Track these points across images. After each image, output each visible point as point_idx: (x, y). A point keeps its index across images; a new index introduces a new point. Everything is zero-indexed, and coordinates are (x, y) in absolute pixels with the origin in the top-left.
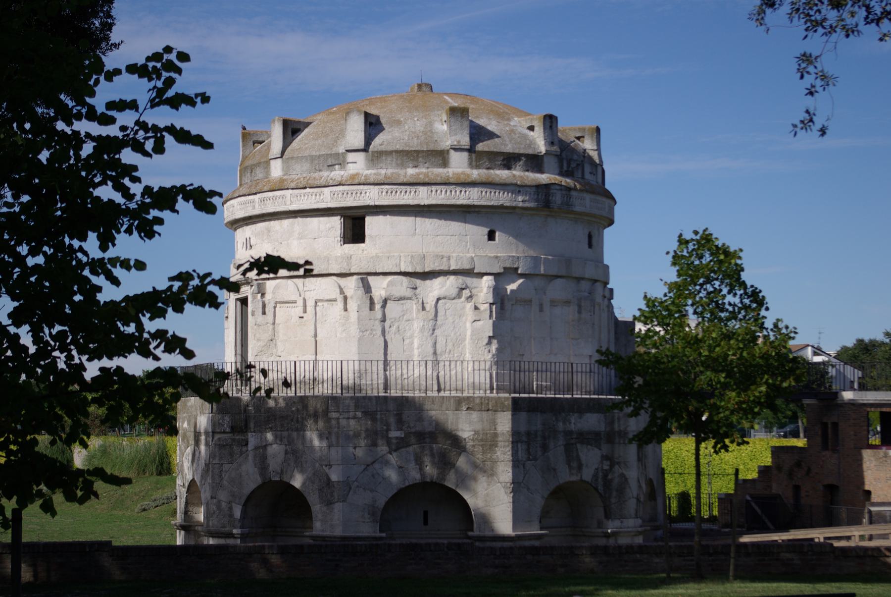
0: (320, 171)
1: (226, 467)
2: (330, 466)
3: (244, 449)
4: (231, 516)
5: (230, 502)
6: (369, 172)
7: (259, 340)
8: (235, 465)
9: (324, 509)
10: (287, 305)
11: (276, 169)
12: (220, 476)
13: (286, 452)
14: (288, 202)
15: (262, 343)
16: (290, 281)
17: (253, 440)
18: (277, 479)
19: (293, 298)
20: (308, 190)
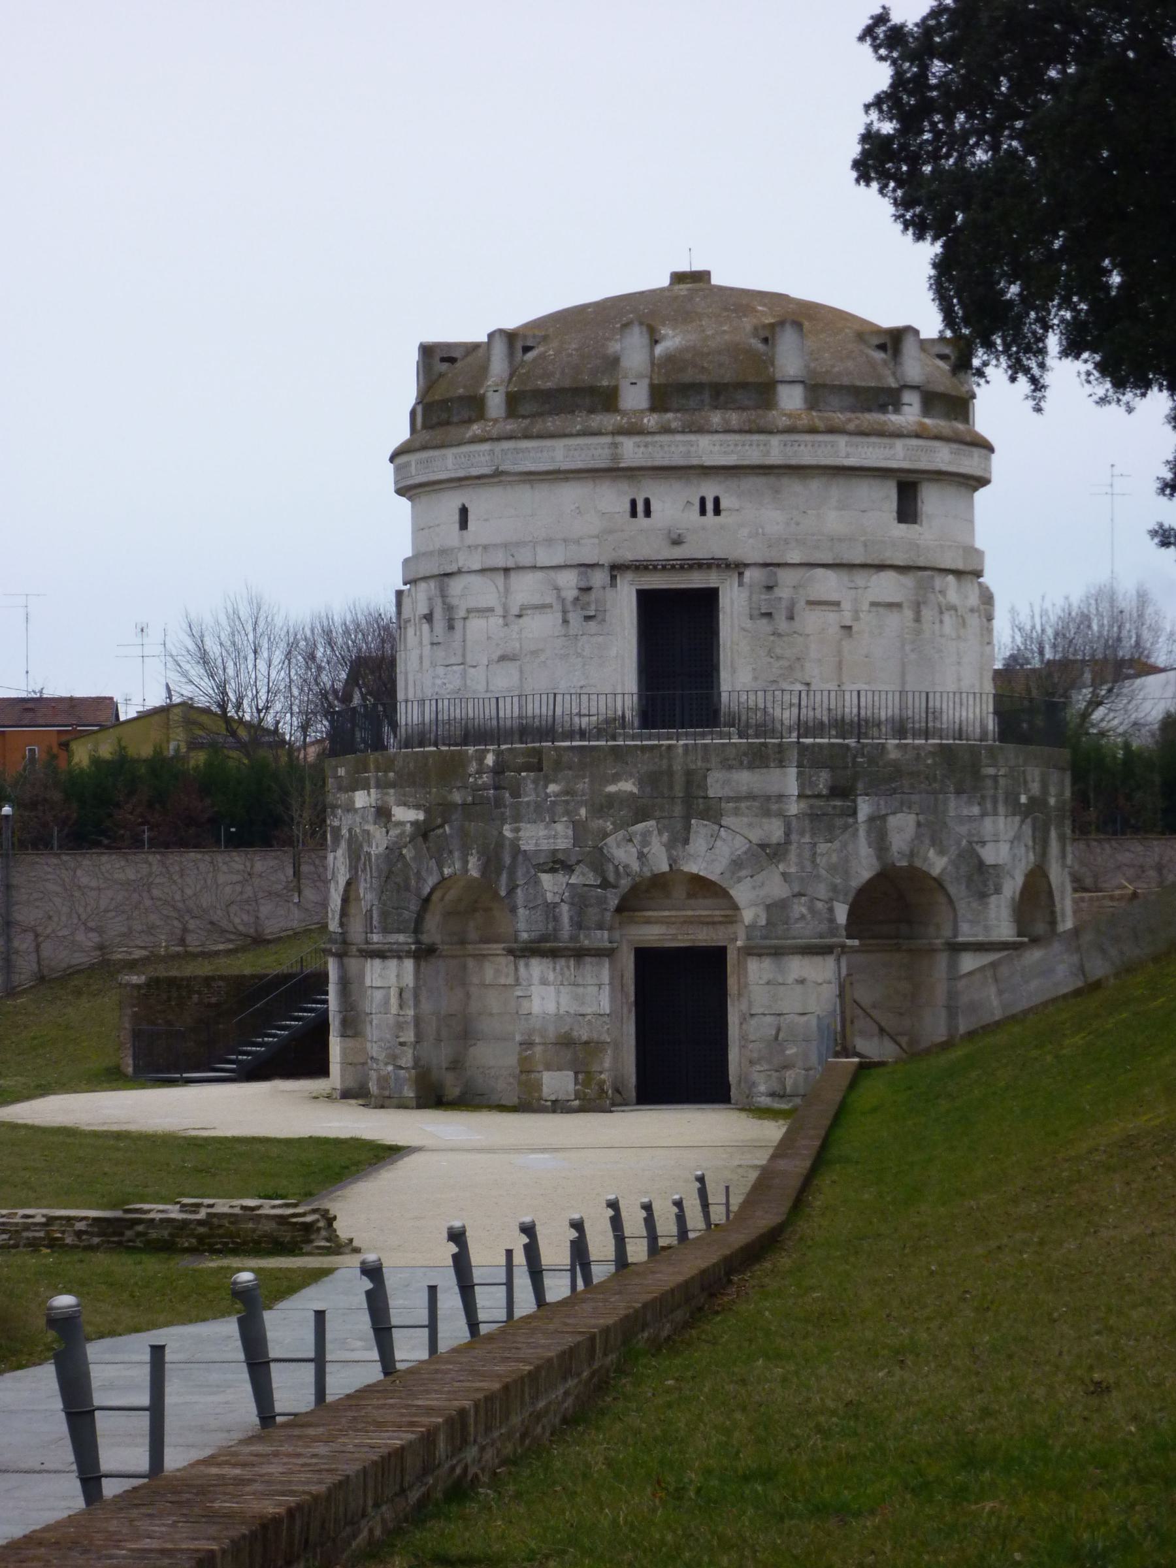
0: (869, 410)
1: (822, 847)
2: (983, 843)
3: (851, 820)
4: (832, 920)
5: (832, 900)
6: (927, 421)
7: (778, 658)
8: (837, 844)
9: (975, 905)
10: (824, 607)
11: (791, 399)
12: (813, 862)
13: (919, 824)
14: (843, 454)
15: (786, 663)
16: (830, 574)
17: (864, 808)
18: (905, 864)
19: (834, 597)
20: (873, 439)
